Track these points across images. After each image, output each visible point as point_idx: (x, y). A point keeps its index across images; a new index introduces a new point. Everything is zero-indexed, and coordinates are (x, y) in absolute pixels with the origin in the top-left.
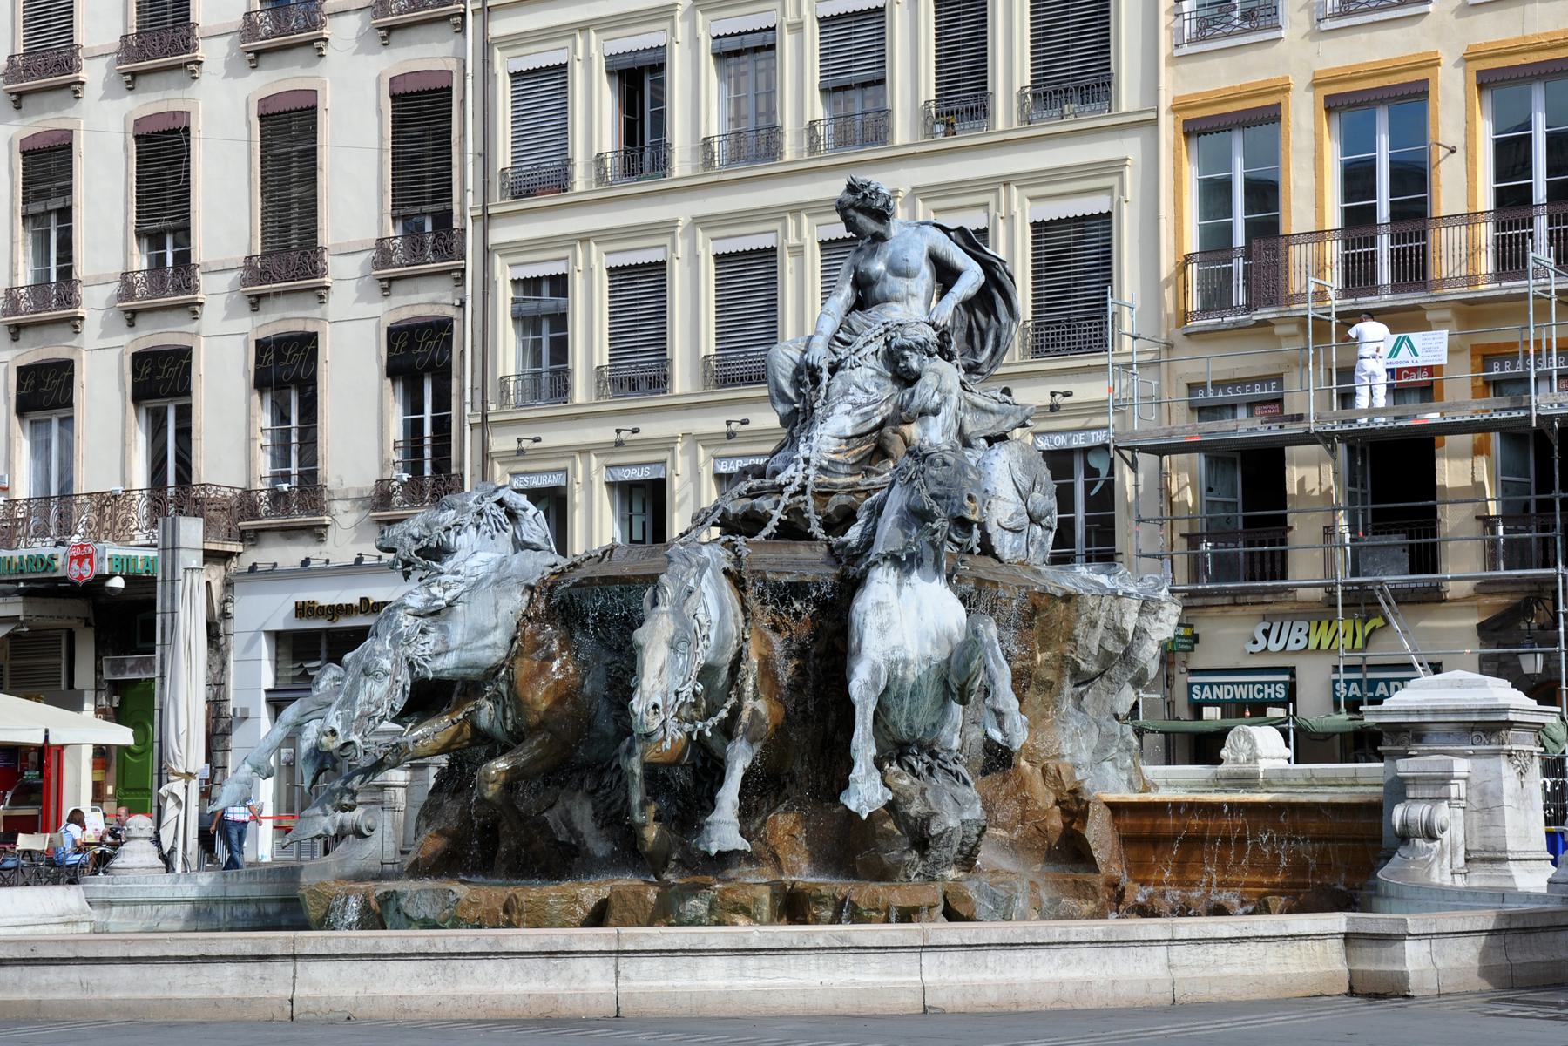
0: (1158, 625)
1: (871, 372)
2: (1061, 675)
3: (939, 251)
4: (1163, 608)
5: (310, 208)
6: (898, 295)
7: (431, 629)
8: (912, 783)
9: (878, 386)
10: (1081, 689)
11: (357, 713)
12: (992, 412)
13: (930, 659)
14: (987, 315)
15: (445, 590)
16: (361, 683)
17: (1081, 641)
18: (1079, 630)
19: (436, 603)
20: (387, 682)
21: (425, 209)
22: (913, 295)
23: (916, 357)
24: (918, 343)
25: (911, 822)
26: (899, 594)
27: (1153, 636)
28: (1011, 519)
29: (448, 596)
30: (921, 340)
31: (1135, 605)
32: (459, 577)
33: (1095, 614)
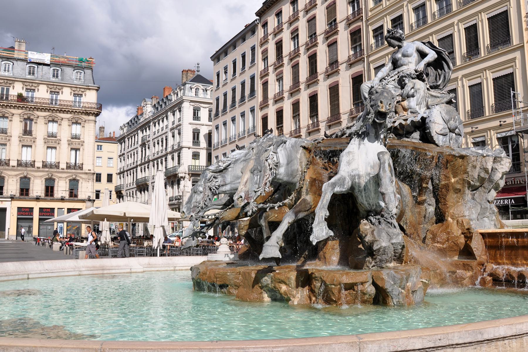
0: (501, 166)
1: (392, 86)
2: (464, 187)
3: (420, 48)
4: (503, 160)
5: (338, 105)
6: (405, 63)
7: (219, 177)
8: (371, 228)
9: (395, 91)
10: (474, 192)
11: (192, 206)
12: (438, 97)
13: (370, 174)
14: (441, 70)
15: (224, 163)
16: (193, 195)
17: (470, 173)
18: (469, 170)
19: (220, 168)
20: (202, 195)
21: (359, 101)
22: (410, 63)
23: (407, 79)
24: (408, 74)
25: (367, 244)
26: (359, 148)
27: (499, 170)
28: (441, 130)
29: (224, 165)
30: (409, 73)
31: (491, 159)
32: (228, 159)
33: (475, 163)
